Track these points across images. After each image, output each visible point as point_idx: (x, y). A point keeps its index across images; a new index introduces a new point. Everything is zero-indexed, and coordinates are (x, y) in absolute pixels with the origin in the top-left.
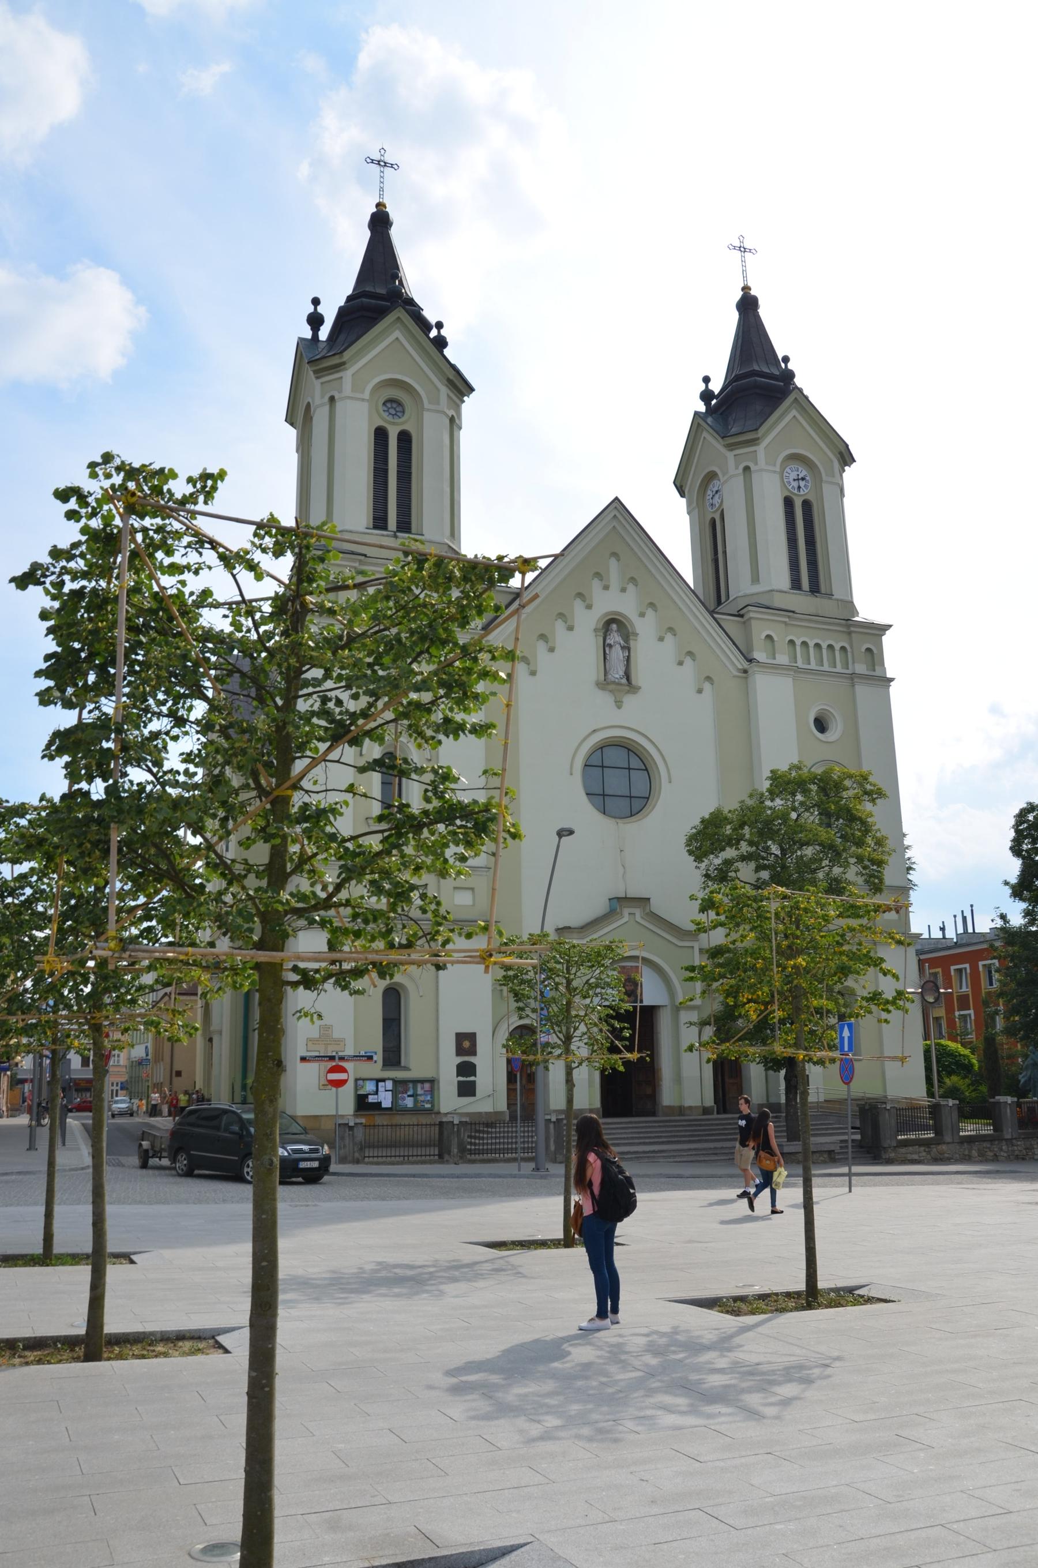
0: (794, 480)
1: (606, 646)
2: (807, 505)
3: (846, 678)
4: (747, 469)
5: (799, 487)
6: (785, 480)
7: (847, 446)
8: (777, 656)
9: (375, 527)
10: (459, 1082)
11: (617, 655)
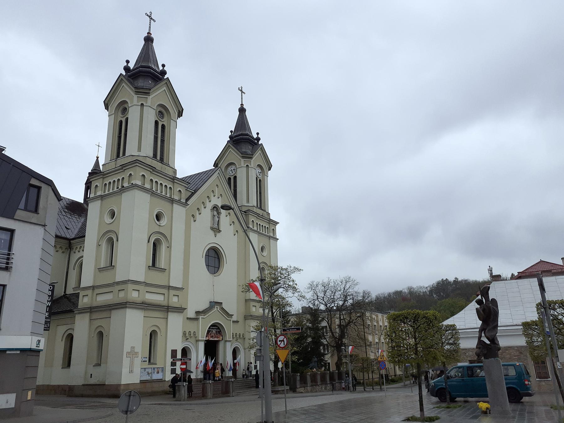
1: (214, 216)
2: (260, 180)
4: (247, 166)
9: (153, 157)
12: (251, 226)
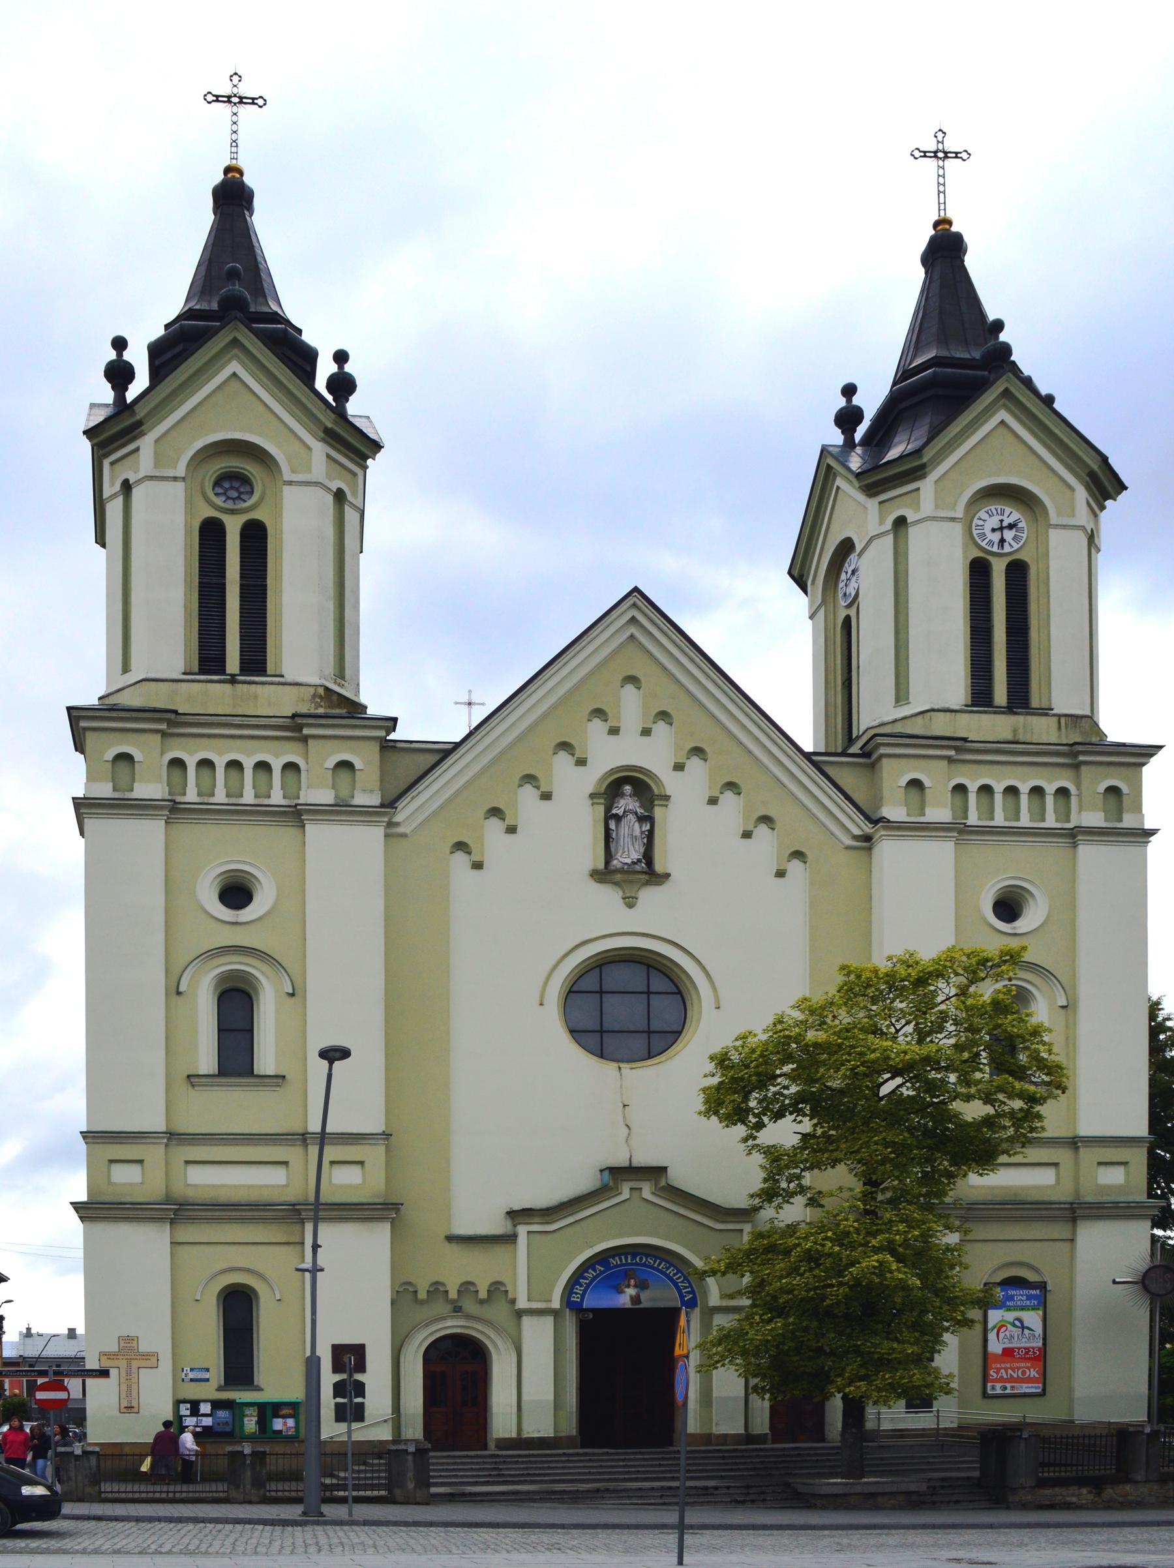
0: (993, 530)
3: (1061, 835)
5: (1002, 541)
6: (975, 532)
7: (1105, 459)
8: (928, 810)
10: (337, 1405)
11: (631, 829)
12: (894, 811)
